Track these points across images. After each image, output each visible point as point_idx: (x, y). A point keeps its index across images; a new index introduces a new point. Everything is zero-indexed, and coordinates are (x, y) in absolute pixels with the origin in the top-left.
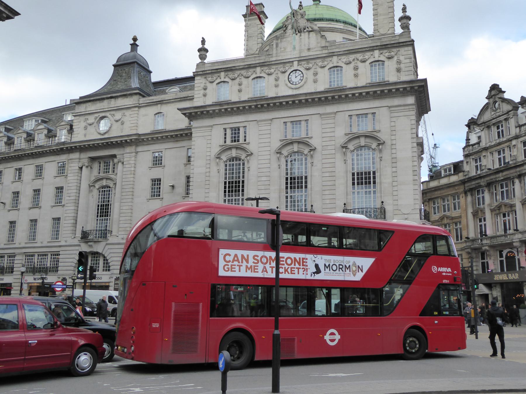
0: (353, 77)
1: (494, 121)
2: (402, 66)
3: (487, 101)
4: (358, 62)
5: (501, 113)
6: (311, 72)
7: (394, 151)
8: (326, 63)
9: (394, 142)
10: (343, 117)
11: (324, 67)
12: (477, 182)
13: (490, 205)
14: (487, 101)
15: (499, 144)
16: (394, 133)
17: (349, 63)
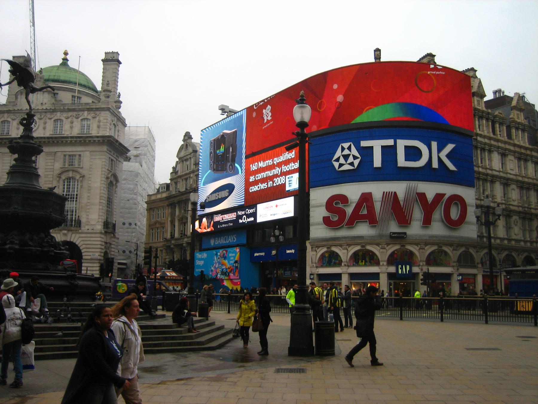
0: (69, 128)
1: (185, 158)
2: (101, 124)
3: (183, 143)
4: (74, 118)
5: (187, 153)
6: (42, 121)
7: (90, 182)
8: (52, 116)
9: (90, 176)
10: (60, 155)
11: (51, 119)
12: (173, 199)
13: (178, 216)
14: (183, 143)
15: (186, 174)
16: (91, 170)
17: (68, 118)
